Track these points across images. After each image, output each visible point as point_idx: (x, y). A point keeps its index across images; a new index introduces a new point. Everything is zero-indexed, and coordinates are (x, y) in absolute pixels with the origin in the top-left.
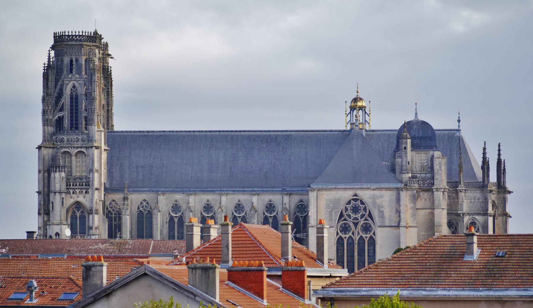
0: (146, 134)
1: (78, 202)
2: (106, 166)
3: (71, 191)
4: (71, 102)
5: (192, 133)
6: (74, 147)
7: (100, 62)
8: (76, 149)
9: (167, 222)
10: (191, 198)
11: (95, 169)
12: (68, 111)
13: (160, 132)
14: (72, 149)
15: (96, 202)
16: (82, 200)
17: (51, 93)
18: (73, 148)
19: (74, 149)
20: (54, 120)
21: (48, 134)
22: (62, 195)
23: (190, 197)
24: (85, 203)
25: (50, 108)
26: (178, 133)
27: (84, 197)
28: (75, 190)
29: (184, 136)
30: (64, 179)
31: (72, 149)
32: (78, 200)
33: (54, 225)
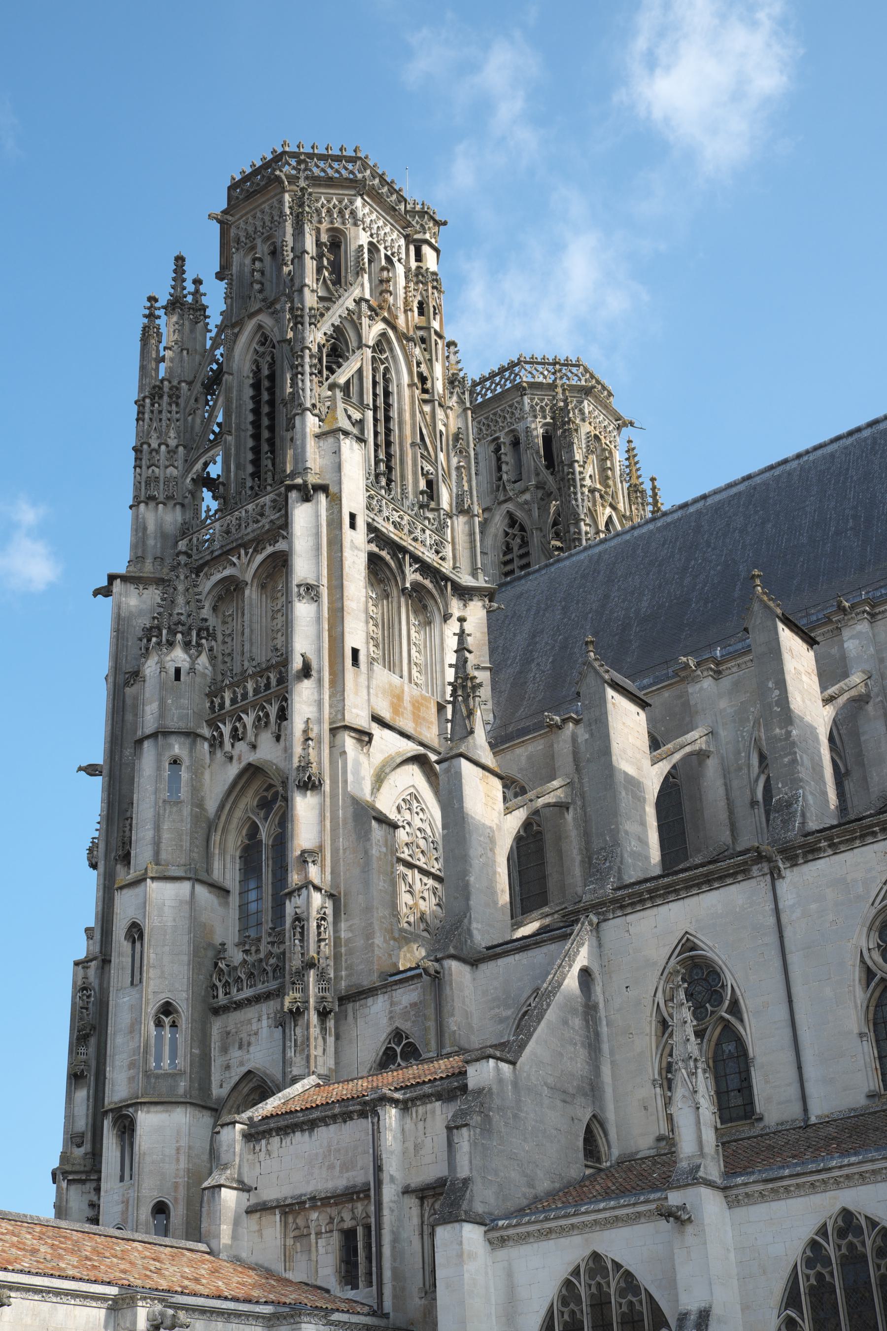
0: (679, 514)
1: (250, 765)
2: (488, 658)
3: (226, 730)
4: (256, 399)
5: (866, 433)
7: (425, 284)
8: (256, 551)
9: (754, 803)
10: (851, 638)
11: (295, 581)
12: (238, 428)
13: (730, 486)
14: (239, 558)
15: (305, 731)
16: (268, 757)
18: (242, 552)
19: (246, 554)
20: (188, 480)
21: (155, 538)
22: (171, 746)
23: (846, 633)
24: (282, 765)
25: (172, 443)
26: (806, 458)
27: (278, 738)
28: (240, 719)
29: (832, 455)
31: (239, 558)
32: (252, 757)
33: (125, 891)
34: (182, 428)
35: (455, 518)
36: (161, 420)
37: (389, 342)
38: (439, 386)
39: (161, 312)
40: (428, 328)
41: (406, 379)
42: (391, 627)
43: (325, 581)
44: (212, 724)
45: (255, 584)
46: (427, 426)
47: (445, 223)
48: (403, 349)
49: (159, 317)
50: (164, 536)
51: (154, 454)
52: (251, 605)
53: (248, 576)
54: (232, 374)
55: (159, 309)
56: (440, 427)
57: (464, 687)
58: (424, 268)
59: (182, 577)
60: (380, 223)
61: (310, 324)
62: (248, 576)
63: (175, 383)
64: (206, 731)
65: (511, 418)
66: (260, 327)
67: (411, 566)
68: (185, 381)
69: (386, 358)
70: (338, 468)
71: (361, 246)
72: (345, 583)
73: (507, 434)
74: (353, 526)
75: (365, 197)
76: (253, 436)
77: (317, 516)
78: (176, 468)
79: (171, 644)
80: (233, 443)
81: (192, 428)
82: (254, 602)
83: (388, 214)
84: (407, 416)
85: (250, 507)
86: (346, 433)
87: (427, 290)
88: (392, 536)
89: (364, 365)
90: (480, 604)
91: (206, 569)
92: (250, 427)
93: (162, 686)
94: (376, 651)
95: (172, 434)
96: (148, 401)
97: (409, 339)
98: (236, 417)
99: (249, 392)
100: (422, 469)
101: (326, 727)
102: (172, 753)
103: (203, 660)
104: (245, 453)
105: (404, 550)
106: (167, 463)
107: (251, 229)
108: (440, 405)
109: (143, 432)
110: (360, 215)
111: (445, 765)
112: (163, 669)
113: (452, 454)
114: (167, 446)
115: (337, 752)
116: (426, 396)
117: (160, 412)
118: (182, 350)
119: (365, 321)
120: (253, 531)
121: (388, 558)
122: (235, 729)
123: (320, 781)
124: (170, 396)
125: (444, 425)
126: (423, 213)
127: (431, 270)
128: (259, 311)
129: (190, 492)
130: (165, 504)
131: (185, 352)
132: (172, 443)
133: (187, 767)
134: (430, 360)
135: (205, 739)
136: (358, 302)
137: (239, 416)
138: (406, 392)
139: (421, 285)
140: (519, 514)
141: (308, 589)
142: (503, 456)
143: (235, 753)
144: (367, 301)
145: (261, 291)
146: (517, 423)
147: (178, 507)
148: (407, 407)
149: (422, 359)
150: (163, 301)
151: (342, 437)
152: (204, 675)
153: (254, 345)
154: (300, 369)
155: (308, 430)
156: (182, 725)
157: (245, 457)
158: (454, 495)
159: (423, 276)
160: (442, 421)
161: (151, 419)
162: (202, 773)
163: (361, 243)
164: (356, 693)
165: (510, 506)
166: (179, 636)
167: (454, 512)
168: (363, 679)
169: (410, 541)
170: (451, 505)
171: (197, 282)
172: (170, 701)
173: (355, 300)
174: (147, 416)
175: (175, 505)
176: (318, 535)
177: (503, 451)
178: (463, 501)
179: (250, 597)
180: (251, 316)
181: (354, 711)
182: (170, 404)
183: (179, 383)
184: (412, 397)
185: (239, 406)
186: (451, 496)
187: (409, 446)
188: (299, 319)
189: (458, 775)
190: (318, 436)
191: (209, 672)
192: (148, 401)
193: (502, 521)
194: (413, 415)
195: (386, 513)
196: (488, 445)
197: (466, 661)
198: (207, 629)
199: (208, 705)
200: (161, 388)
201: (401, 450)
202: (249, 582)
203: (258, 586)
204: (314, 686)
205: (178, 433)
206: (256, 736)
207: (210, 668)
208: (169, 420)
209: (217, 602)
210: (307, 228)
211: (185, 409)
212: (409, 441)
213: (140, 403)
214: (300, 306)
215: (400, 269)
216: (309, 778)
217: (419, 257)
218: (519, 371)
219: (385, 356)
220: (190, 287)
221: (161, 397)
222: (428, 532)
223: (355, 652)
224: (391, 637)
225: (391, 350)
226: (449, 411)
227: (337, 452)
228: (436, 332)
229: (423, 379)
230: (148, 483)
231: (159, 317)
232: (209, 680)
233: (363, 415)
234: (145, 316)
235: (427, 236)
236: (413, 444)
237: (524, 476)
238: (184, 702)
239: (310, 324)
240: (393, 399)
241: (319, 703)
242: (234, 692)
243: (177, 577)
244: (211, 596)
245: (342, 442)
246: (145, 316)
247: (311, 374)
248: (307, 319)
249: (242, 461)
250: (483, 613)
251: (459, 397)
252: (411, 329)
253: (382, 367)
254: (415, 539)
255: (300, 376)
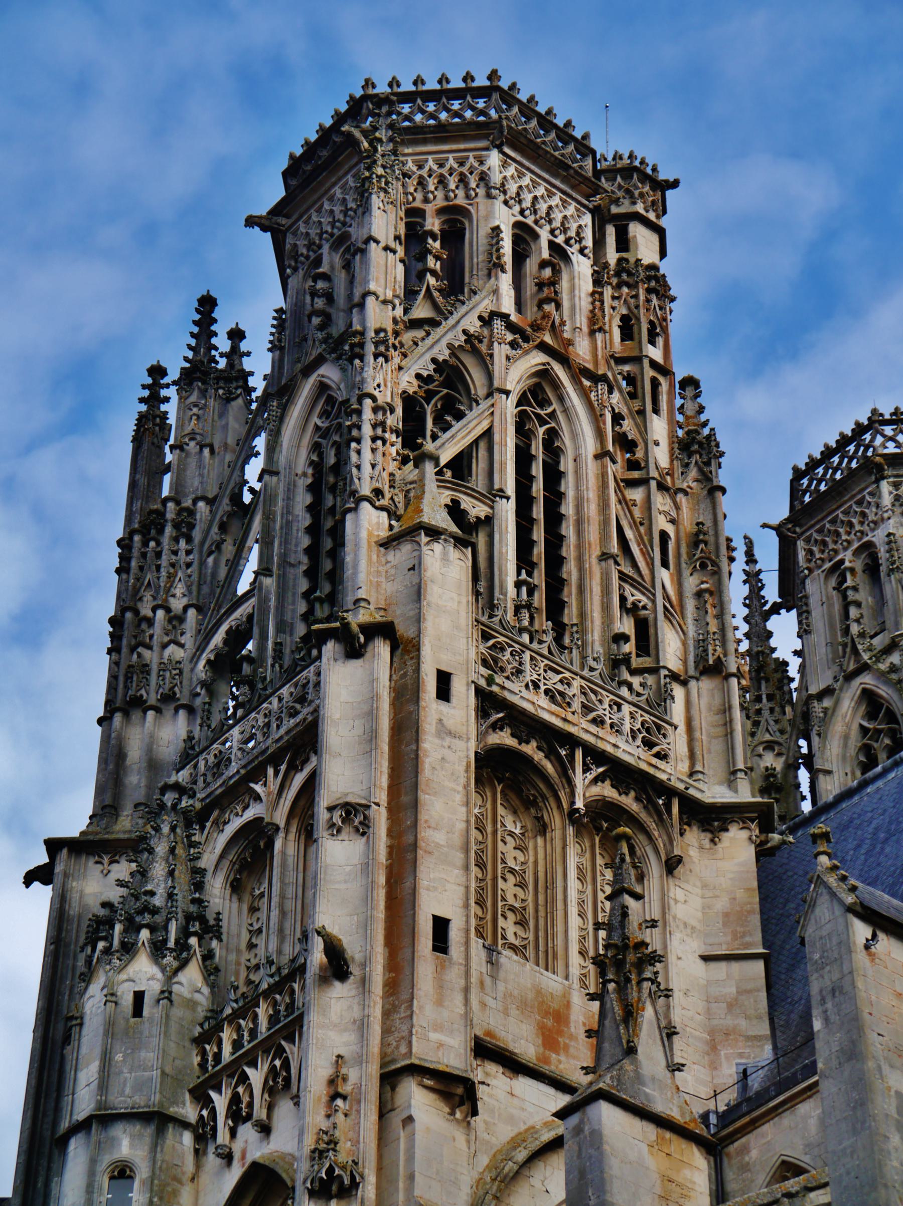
1: (255, 1165)
2: (758, 937)
6: (275, 760)
17: (191, 512)
19: (276, 773)
20: (202, 663)
22: (114, 1143)
28: (244, 1078)
30: (146, 1012)
31: (265, 785)
34: (195, 577)
35: (693, 684)
36: (158, 568)
37: (556, 386)
38: (661, 456)
39: (171, 392)
40: (637, 360)
41: (590, 446)
42: (550, 885)
43: (382, 797)
44: (201, 1096)
45: (293, 829)
46: (635, 525)
47: (675, 184)
48: (584, 394)
49: (167, 400)
50: (153, 765)
51: (144, 626)
52: (284, 864)
53: (280, 817)
54: (277, 473)
55: (167, 386)
56: (661, 523)
57: (619, 965)
58: (632, 260)
59: (166, 829)
60: (541, 191)
61: (376, 356)
62: (280, 817)
63: (187, 503)
64: (190, 1111)
65: (862, 523)
66: (322, 387)
67: (586, 769)
68: (203, 498)
69: (553, 415)
70: (418, 593)
71: (496, 230)
72: (422, 796)
73: (856, 553)
74: (444, 692)
75: (507, 150)
76: (307, 573)
77: (373, 681)
78: (182, 646)
79: (128, 949)
80: (273, 589)
81: (214, 574)
82: (291, 861)
83: (555, 175)
84: (592, 509)
85: (285, 691)
86: (434, 533)
87: (636, 297)
88: (546, 716)
89: (496, 424)
90: (744, 834)
91: (216, 813)
92: (305, 560)
93: (109, 1028)
94: (521, 933)
95: (179, 589)
96: (137, 538)
97: (596, 379)
98: (280, 544)
99: (303, 499)
100: (623, 599)
101: (374, 1070)
102: (116, 1156)
103: (192, 975)
104: (294, 603)
105: (572, 741)
106: (166, 639)
107: (313, 232)
108: (662, 487)
109: (127, 590)
110: (496, 178)
111: (574, 1120)
112: (111, 997)
113: (686, 572)
114: (168, 610)
115: (396, 1119)
116: (636, 474)
117: (158, 555)
118: (202, 447)
119: (500, 351)
120: (287, 733)
121: (538, 757)
122: (235, 1099)
123: (353, 1177)
124: (176, 526)
125: (673, 521)
126: (628, 172)
127: (645, 262)
128: (319, 361)
129: (203, 684)
130: (158, 710)
131: (206, 451)
132: (177, 604)
133: (143, 1182)
134: (641, 412)
135: (185, 1125)
136: (486, 321)
137: (285, 542)
138: (591, 468)
139: (625, 290)
140: (884, 691)
141: (348, 813)
142: (850, 593)
143: (237, 1147)
144: (505, 317)
145: (321, 327)
146: (873, 530)
147: (182, 713)
148: (592, 494)
149: (625, 411)
150: (174, 374)
151: (424, 539)
152: (191, 1004)
153: (315, 420)
154: (355, 433)
155: (364, 534)
156: (140, 1101)
157: (294, 611)
158: (691, 643)
159: (630, 274)
160: (665, 513)
161: (141, 568)
162: (175, 1193)
163: (497, 223)
164: (439, 1002)
165: (867, 680)
166: (145, 934)
167: (692, 672)
168: (454, 976)
169: (585, 725)
170: (685, 662)
171: (236, 335)
172: (119, 1057)
173: (480, 318)
174: (134, 563)
175: (176, 711)
176: (372, 715)
177: (849, 582)
178: (706, 651)
179: (283, 853)
180: (307, 371)
181: (434, 1036)
182: (176, 540)
183: (195, 502)
184: (603, 477)
185: (288, 525)
186: (684, 644)
187: (594, 560)
188: (357, 350)
189: (596, 1137)
190: (386, 544)
191: (203, 998)
192: (137, 538)
193: (855, 710)
194: (604, 505)
195: (529, 675)
196: (827, 578)
197: (625, 914)
198: (202, 919)
199: (197, 1060)
200: (161, 514)
201: (581, 569)
202: (282, 825)
203: (299, 831)
204: (353, 993)
205: (189, 587)
206: (270, 1108)
207: (206, 990)
208: (173, 565)
209: (239, 871)
210: (376, 201)
211: (202, 543)
212: (596, 552)
213: (124, 544)
214: (359, 328)
215: (583, 267)
216: (330, 1170)
217: (623, 243)
218: (873, 439)
219: (550, 410)
220: (222, 343)
221: (161, 531)
222: (626, 708)
223: (441, 926)
224: (550, 902)
225: (561, 399)
226: (680, 497)
227: (416, 568)
228: (653, 364)
229: (626, 443)
230: (128, 678)
231: (167, 400)
232: (201, 1013)
233: (492, 508)
234: (142, 400)
235: (640, 208)
236: (605, 557)
237: (889, 624)
238: (149, 1056)
239: (376, 356)
240: (567, 483)
241: (362, 1026)
242: (239, 1029)
243: (157, 829)
244: (226, 864)
245: (425, 549)
246: (142, 400)
247: (374, 439)
248: (370, 348)
249: (288, 617)
250: (748, 853)
251: (700, 470)
252: (602, 362)
253: (541, 431)
254: (598, 722)
255: (354, 445)
